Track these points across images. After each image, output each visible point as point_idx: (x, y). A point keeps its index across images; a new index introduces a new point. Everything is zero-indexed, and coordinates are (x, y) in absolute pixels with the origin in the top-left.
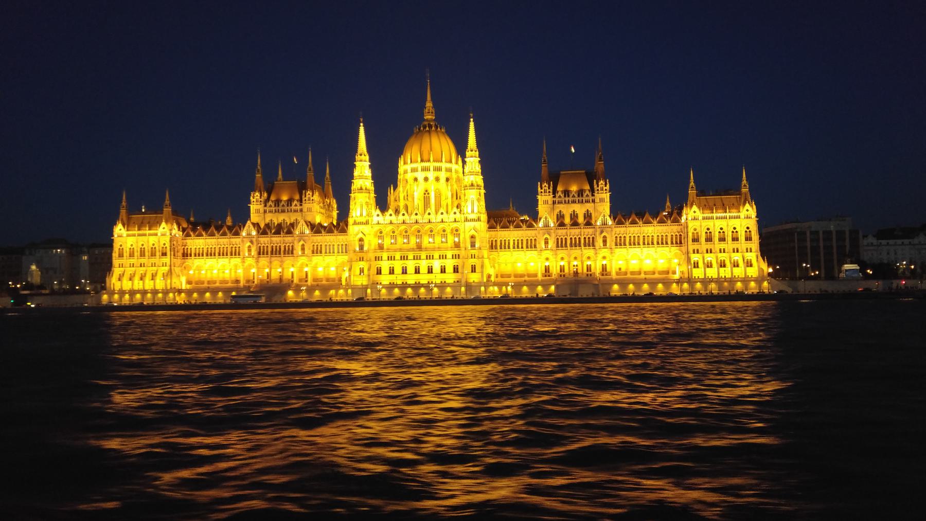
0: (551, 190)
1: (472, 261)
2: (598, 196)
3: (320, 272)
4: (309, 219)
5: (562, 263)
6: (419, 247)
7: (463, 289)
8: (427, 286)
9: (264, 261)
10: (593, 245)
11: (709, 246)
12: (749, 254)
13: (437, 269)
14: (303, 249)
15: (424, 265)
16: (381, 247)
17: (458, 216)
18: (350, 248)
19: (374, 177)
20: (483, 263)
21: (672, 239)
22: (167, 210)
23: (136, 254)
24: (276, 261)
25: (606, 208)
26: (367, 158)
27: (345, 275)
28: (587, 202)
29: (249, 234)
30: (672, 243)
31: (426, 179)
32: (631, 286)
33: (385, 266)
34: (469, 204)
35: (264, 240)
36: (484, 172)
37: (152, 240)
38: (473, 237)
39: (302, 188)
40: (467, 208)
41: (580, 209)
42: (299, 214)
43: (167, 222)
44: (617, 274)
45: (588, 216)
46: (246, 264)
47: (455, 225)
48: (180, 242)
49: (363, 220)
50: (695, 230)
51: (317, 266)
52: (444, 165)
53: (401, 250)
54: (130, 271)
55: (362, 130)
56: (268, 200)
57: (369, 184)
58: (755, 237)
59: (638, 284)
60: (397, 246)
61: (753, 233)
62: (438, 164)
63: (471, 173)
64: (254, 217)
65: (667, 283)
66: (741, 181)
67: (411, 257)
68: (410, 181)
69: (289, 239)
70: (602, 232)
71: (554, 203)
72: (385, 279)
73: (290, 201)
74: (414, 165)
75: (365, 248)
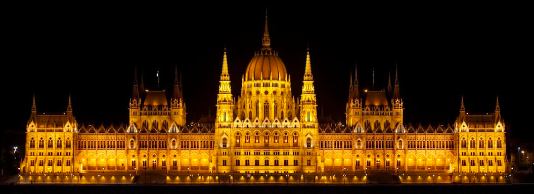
0: (361, 106)
1: (308, 157)
2: (394, 111)
3: (185, 162)
6: (267, 146)
7: (302, 178)
8: (284, 175)
9: (143, 152)
12: (499, 156)
13: (281, 162)
15: (272, 159)
16: (238, 145)
17: (298, 124)
18: (216, 145)
19: (232, 92)
20: (316, 158)
22: (70, 112)
24: (153, 152)
25: (400, 119)
26: (228, 78)
27: (212, 165)
28: (387, 114)
29: (132, 132)
30: (447, 147)
31: (266, 93)
33: (243, 159)
36: (316, 92)
37: (58, 135)
38: (309, 139)
39: (170, 96)
41: (382, 121)
43: (71, 123)
45: (387, 124)
47: (297, 130)
48: (77, 138)
49: (226, 124)
51: (193, 158)
52: (280, 83)
53: (254, 147)
54: (40, 158)
55: (225, 56)
56: (142, 106)
57: (229, 97)
58: (504, 145)
59: (425, 175)
62: (275, 82)
63: (308, 92)
64: (132, 119)
66: (496, 105)
67: (262, 153)
71: (363, 114)
72: (242, 169)
74: (258, 82)
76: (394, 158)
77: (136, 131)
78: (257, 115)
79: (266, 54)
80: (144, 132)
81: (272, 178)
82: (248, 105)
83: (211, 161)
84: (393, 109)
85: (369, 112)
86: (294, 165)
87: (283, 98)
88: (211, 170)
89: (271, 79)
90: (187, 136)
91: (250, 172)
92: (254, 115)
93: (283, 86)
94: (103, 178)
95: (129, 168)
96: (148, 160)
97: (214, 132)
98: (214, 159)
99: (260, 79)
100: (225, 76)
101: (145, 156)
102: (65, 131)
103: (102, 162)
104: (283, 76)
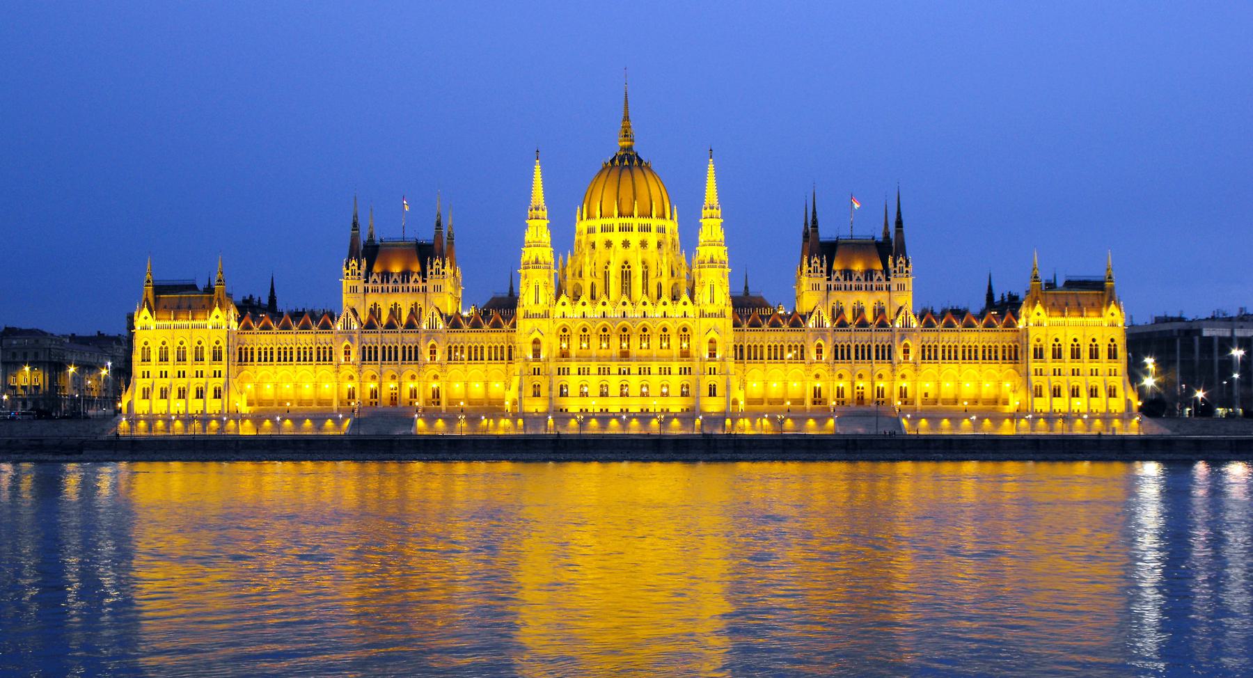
0: (824, 270)
1: (710, 379)
2: (894, 282)
3: (457, 389)
4: (438, 302)
5: (841, 384)
9: (370, 369)
10: (890, 358)
11: (1057, 365)
12: (1112, 378)
14: (433, 352)
16: (564, 355)
17: (690, 308)
18: (518, 353)
21: (1004, 352)
23: (170, 357)
24: (389, 369)
25: (905, 299)
28: (879, 289)
29: (347, 327)
30: (1004, 358)
31: (626, 244)
32: (945, 422)
33: (573, 382)
34: (707, 290)
35: (371, 338)
36: (727, 242)
37: (198, 334)
38: (712, 341)
40: (703, 295)
41: (868, 301)
42: (422, 295)
44: (924, 402)
45: (880, 311)
46: (341, 376)
49: (539, 310)
50: (1038, 340)
52: (655, 223)
53: (598, 359)
57: (546, 254)
58: (1122, 354)
59: (955, 419)
60: (594, 350)
61: (1119, 348)
64: (348, 300)
65: (997, 419)
67: (614, 370)
68: (600, 245)
69: (410, 338)
70: (903, 338)
71: (829, 289)
72: (573, 405)
73: (406, 274)
75: (543, 355)
76: (893, 380)
77: (356, 327)
78: (607, 292)
79: (626, 163)
80: (370, 326)
81: (634, 422)
82: (587, 271)
83: (508, 387)
84: (892, 278)
85: (842, 283)
86: (683, 395)
87: (661, 254)
88: (508, 405)
89: (636, 214)
90: (459, 336)
91: (590, 410)
92: (599, 290)
93: (661, 230)
94: (288, 422)
95: (341, 403)
96: (380, 386)
97: (514, 326)
98: (515, 382)
99: (612, 216)
100: (537, 209)
101: (374, 377)
102: (210, 327)
103: (287, 389)
104: (660, 205)
